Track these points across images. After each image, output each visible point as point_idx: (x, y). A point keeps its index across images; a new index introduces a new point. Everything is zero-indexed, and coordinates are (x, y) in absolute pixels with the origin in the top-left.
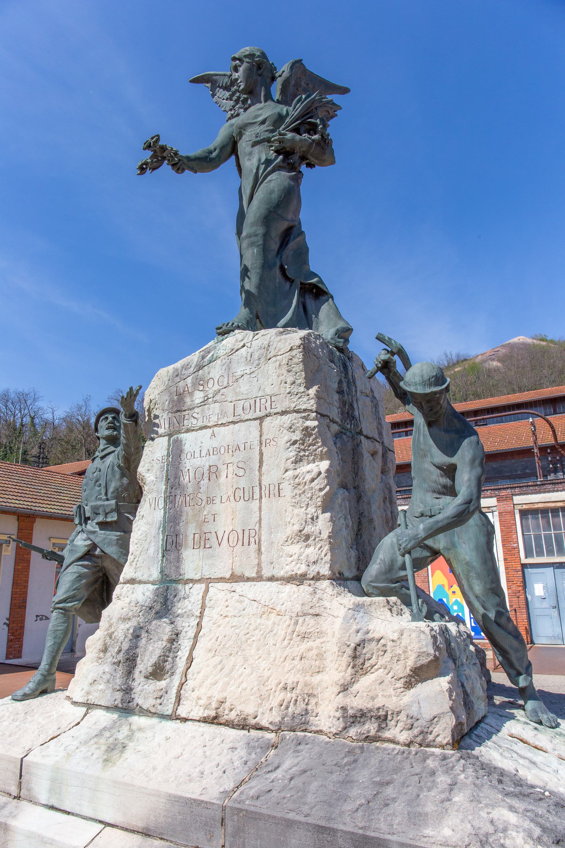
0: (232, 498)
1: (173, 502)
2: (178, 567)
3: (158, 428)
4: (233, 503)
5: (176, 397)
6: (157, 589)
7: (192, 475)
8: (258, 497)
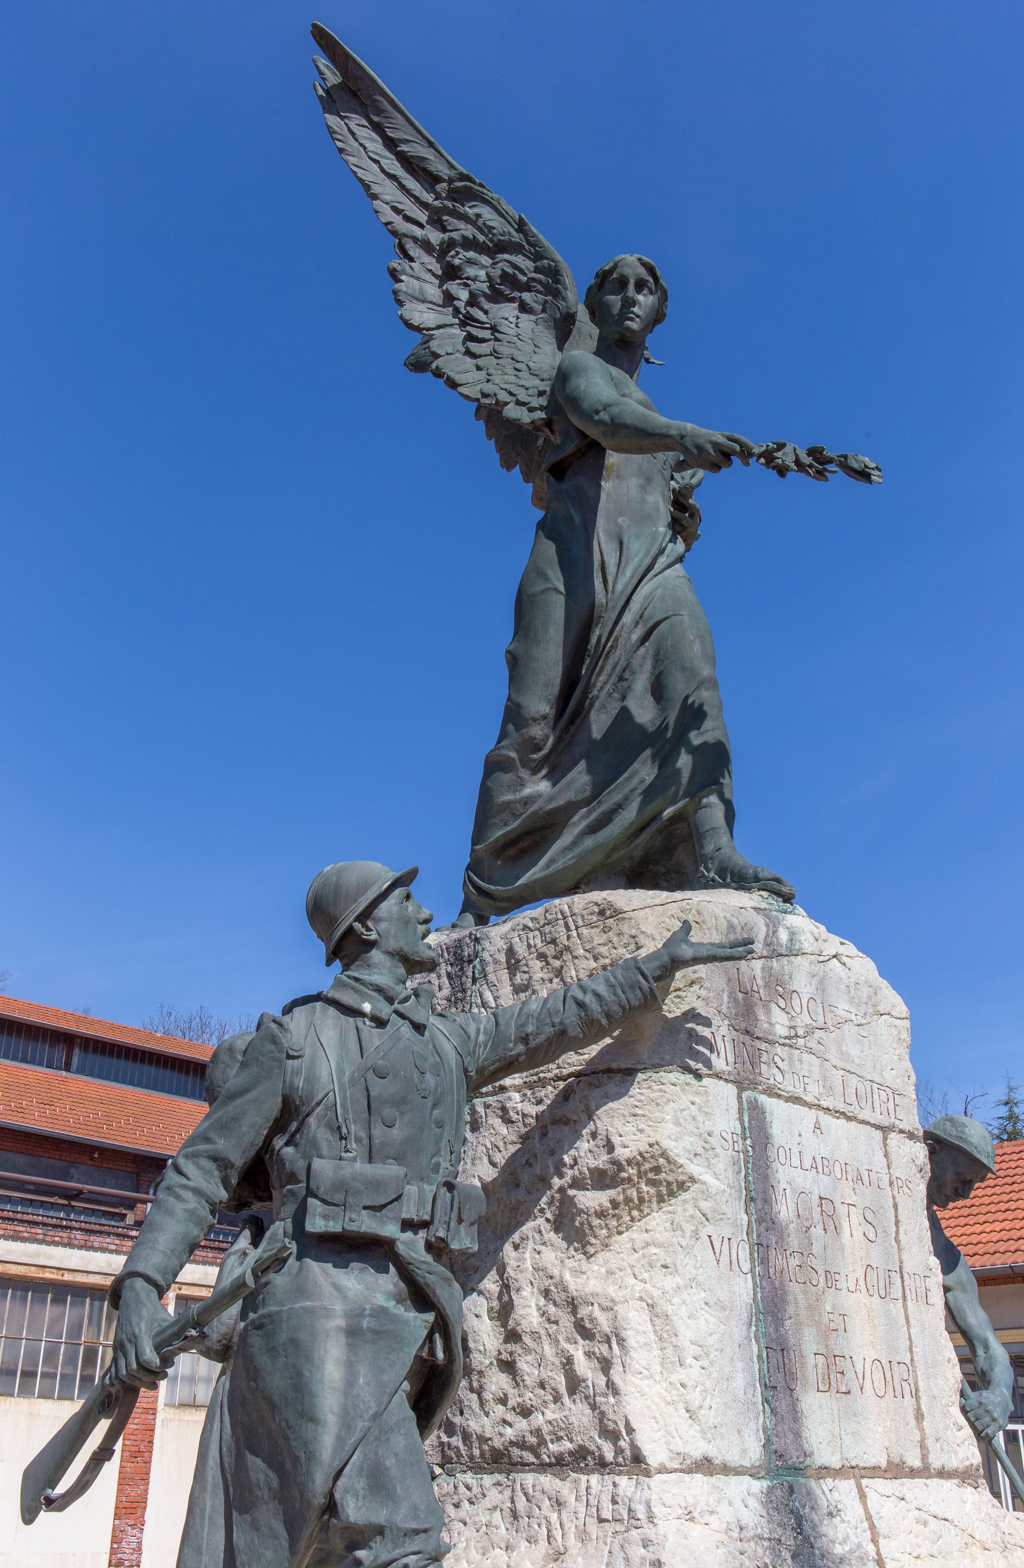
0: (862, 1282)
1: (764, 1262)
2: (798, 1435)
3: (712, 1051)
4: (863, 1298)
5: (740, 995)
6: (770, 1490)
7: (792, 1206)
8: (900, 1295)
